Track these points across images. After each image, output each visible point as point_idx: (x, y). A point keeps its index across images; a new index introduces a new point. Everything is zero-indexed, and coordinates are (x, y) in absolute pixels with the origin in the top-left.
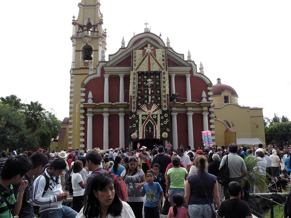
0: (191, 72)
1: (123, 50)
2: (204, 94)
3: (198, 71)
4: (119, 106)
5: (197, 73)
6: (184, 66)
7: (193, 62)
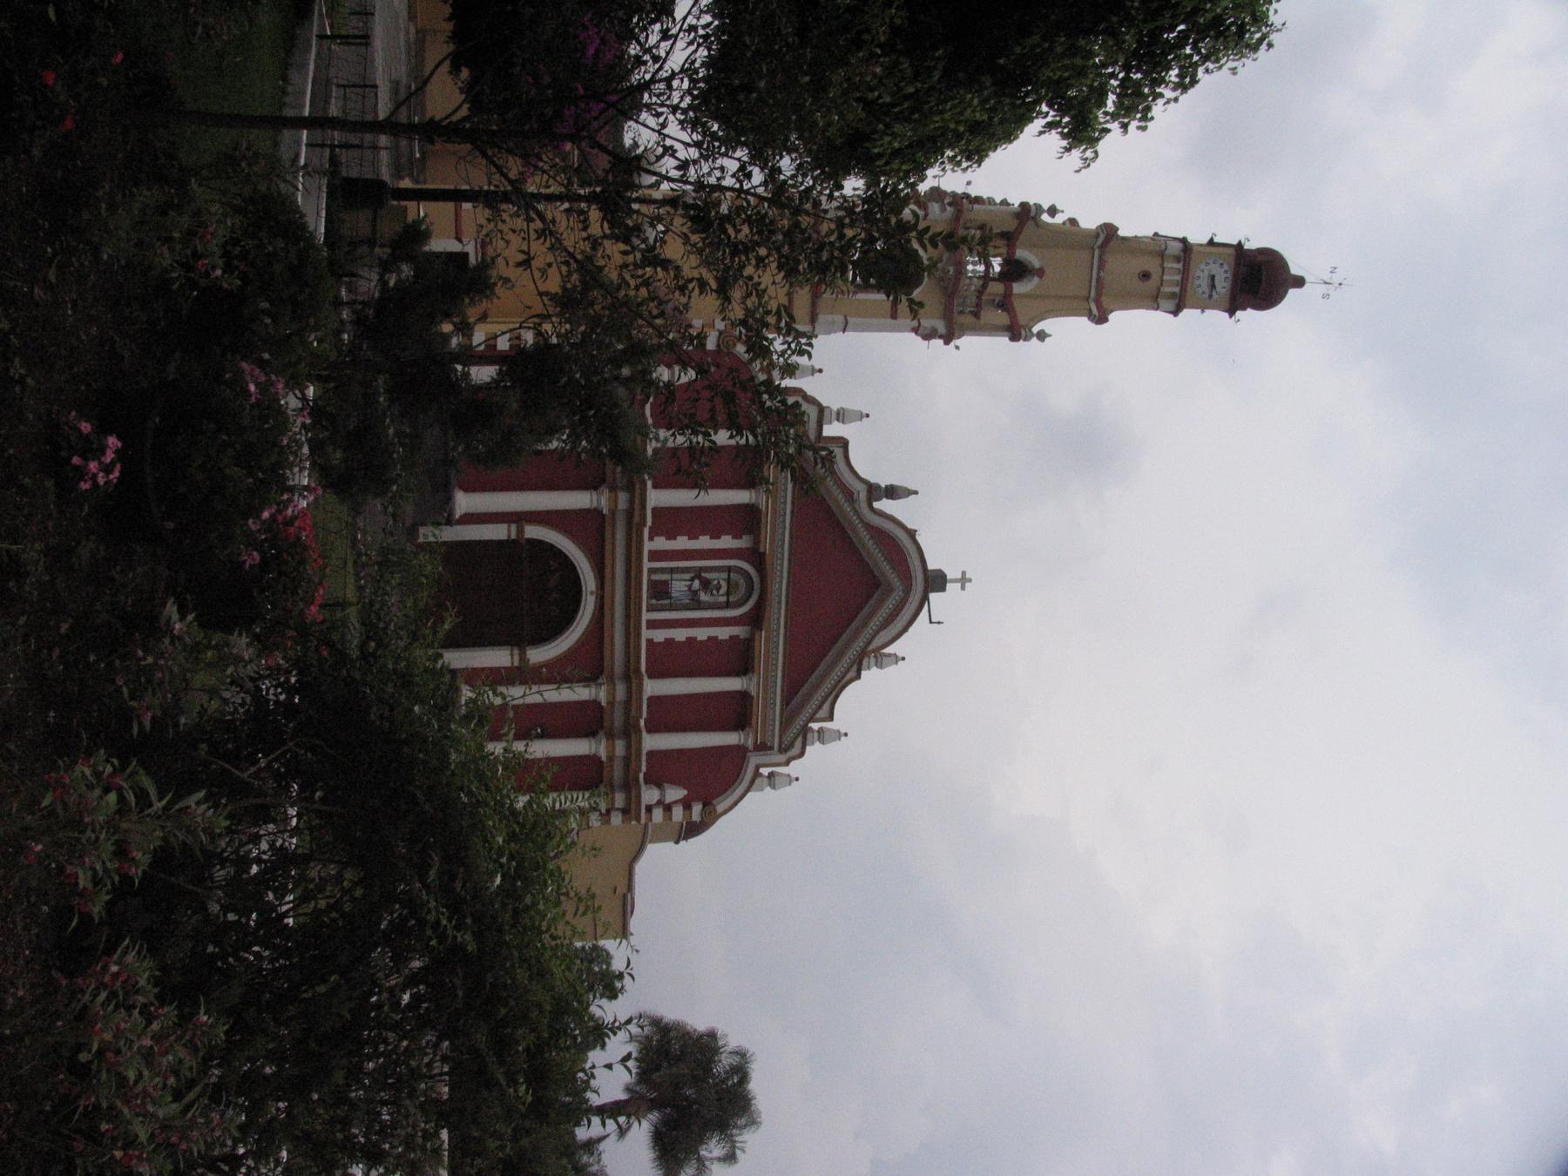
0: (762, 747)
1: (863, 495)
2: (675, 793)
3: (765, 771)
4: (638, 491)
5: (757, 767)
6: (786, 723)
7: (802, 754)
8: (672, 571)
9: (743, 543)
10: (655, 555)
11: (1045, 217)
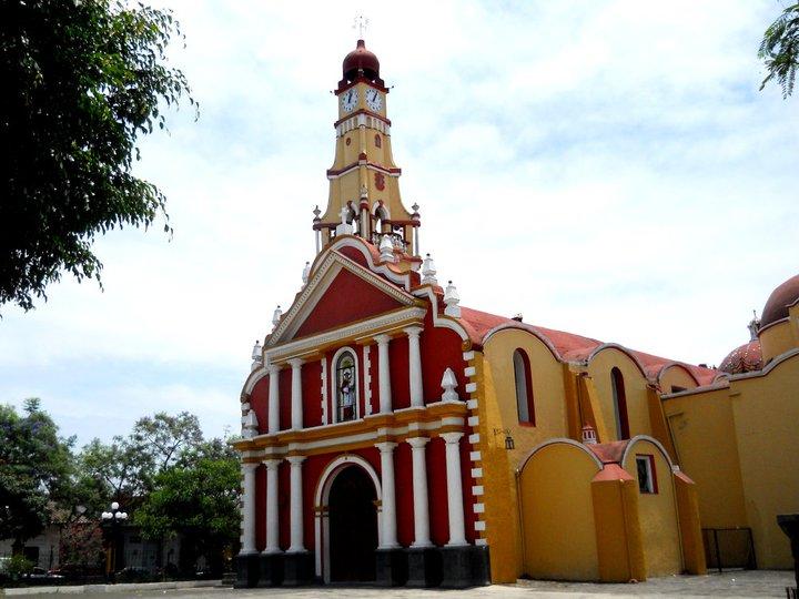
2: (448, 379)
8: (338, 407)
9: (324, 363)
10: (330, 422)
11: (321, 216)
